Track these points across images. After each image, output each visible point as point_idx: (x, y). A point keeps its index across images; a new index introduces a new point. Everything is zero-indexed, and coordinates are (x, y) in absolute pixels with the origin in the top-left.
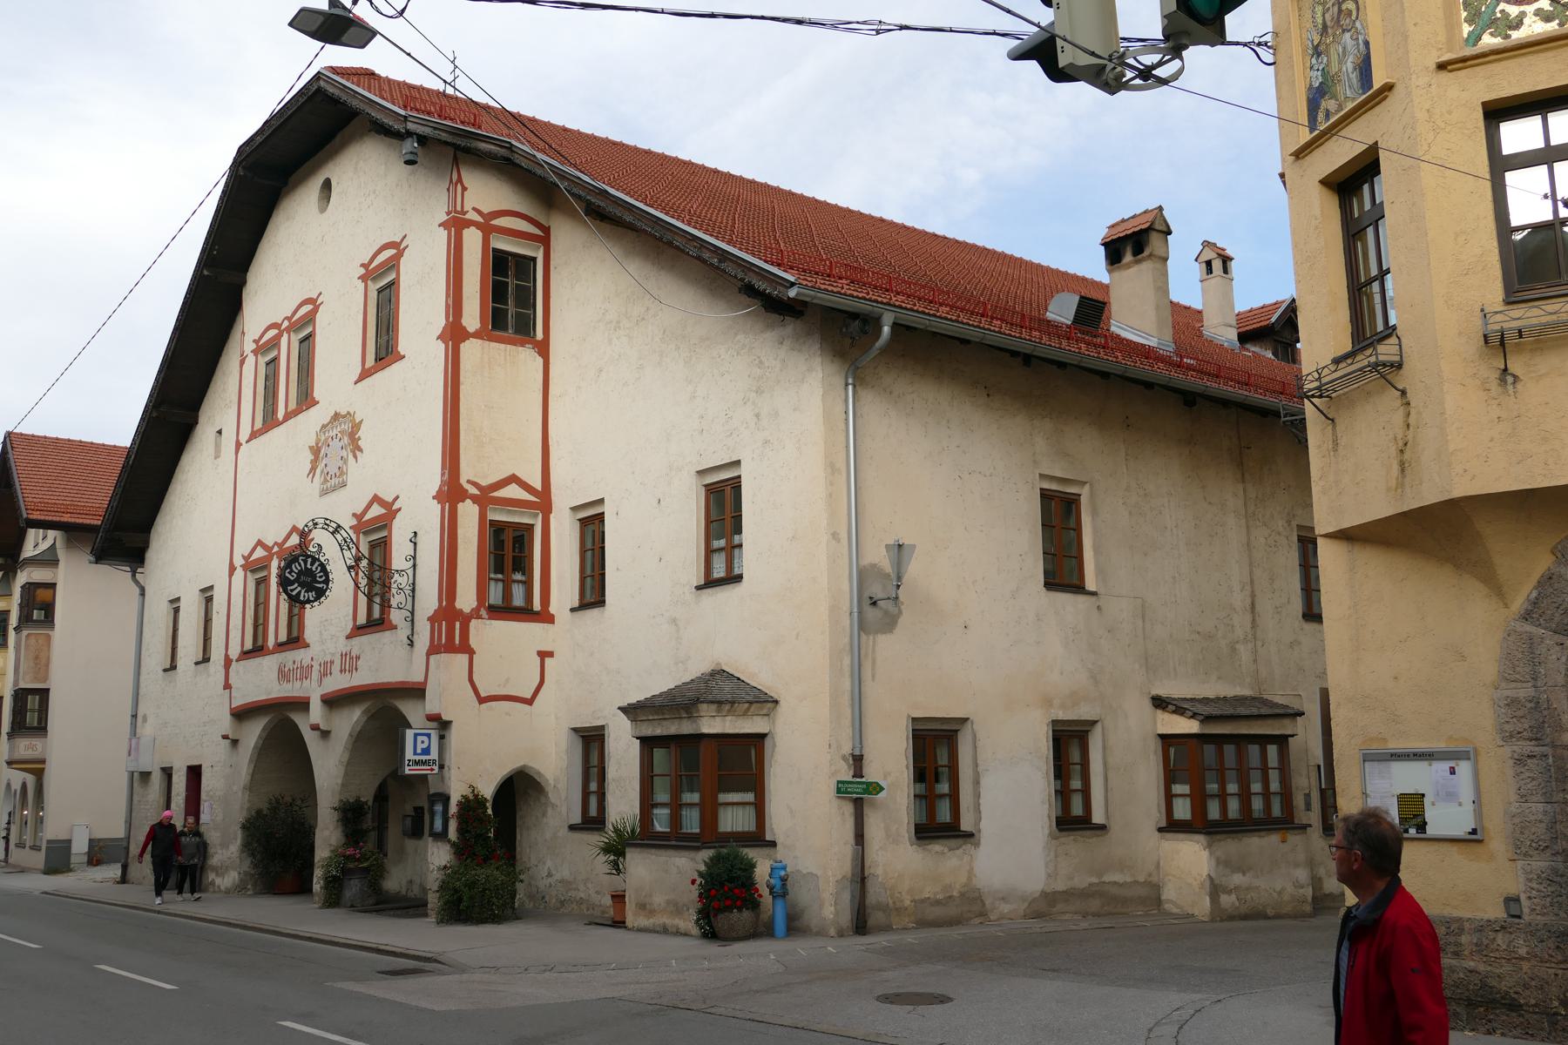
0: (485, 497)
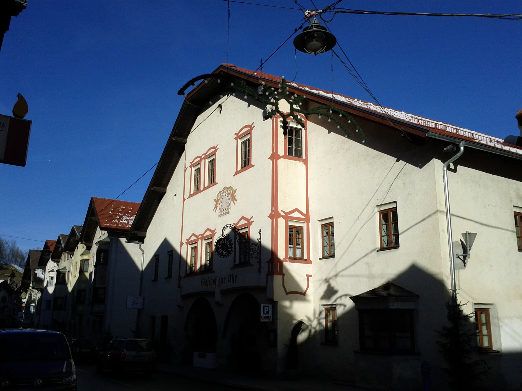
0: (287, 217)
